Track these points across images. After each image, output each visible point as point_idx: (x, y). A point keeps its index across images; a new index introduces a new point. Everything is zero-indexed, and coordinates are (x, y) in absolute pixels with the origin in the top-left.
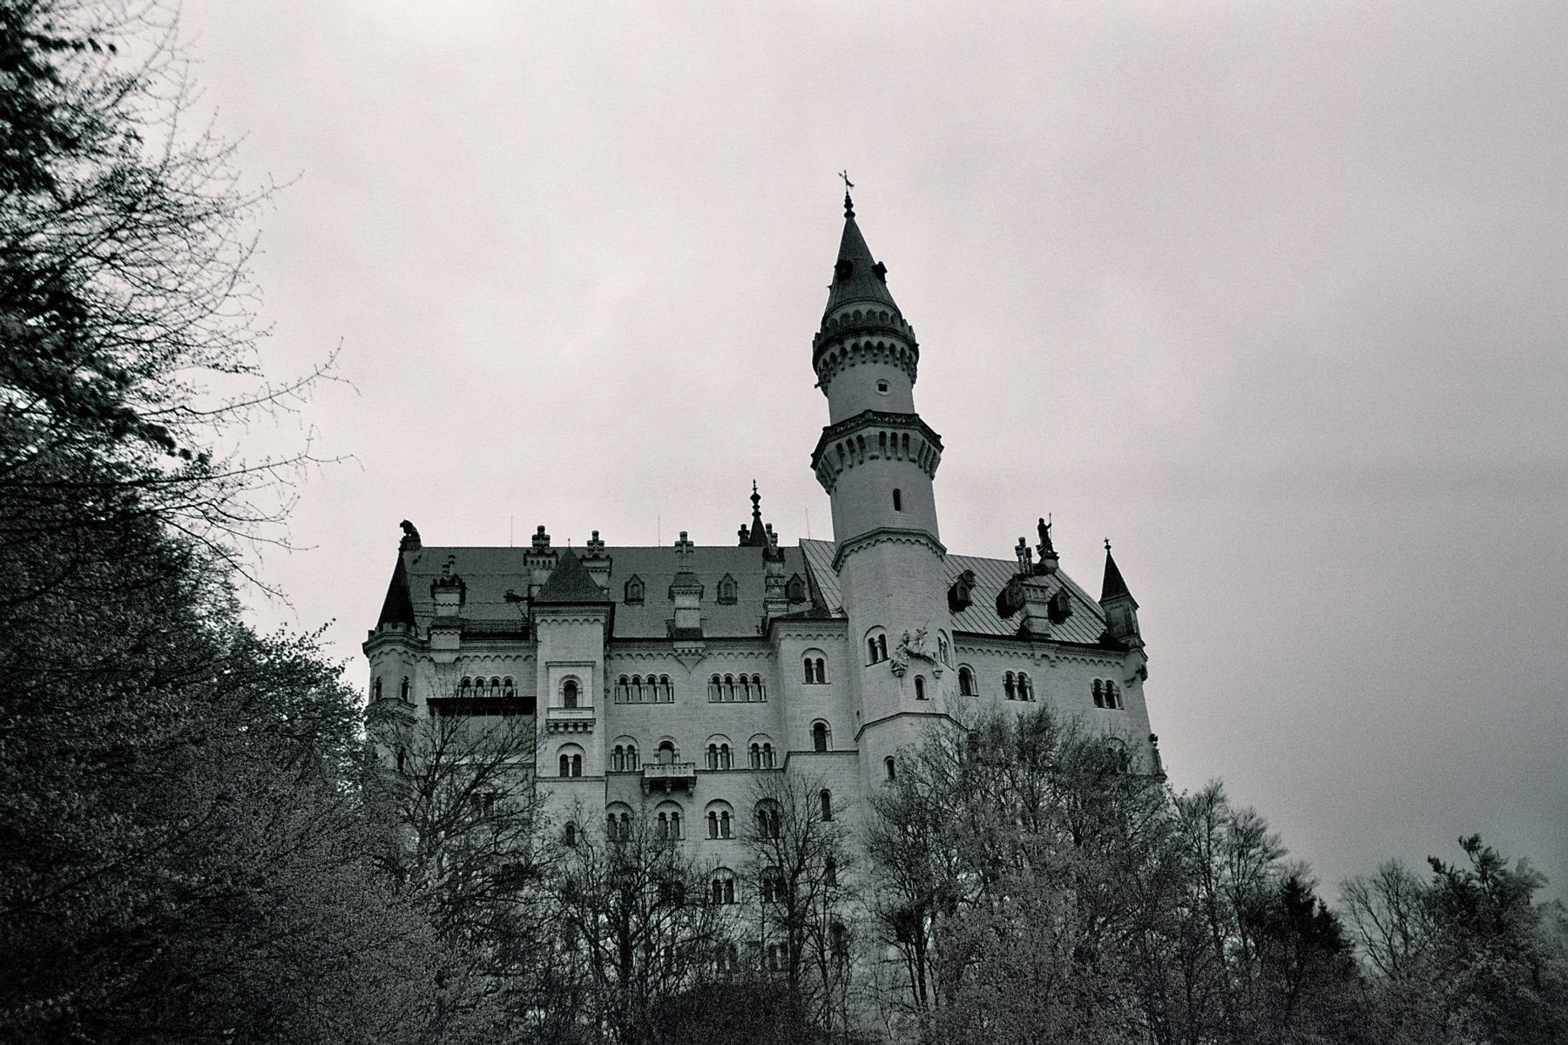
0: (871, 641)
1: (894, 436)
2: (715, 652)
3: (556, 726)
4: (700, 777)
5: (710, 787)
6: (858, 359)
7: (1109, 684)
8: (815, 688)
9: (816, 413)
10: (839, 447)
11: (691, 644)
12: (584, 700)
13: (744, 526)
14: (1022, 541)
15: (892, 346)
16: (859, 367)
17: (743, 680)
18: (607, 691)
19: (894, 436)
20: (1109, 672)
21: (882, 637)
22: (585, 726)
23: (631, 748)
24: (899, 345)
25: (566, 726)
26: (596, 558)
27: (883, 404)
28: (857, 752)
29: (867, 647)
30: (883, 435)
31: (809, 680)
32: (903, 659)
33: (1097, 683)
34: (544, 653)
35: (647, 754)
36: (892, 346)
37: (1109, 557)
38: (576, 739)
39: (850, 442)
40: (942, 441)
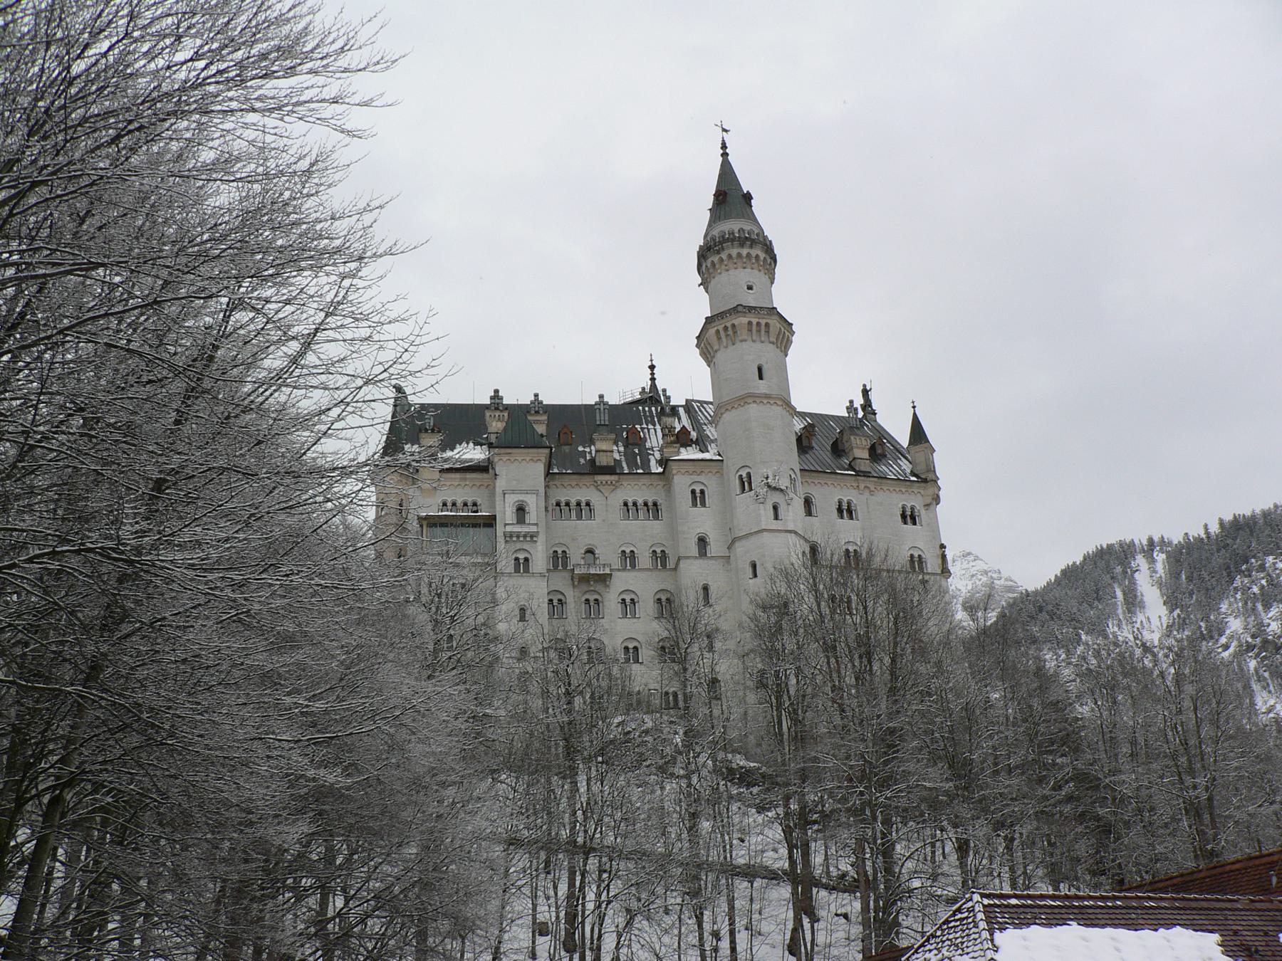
1: (758, 324)
3: (511, 536)
5: (623, 581)
6: (731, 265)
7: (912, 508)
8: (699, 510)
9: (699, 306)
10: (718, 331)
11: (607, 477)
12: (532, 517)
14: (851, 402)
15: (757, 256)
17: (646, 504)
19: (758, 324)
20: (914, 500)
21: (749, 475)
22: (532, 537)
24: (762, 255)
25: (518, 537)
26: (537, 412)
27: (751, 300)
29: (737, 481)
30: (750, 323)
31: (695, 505)
34: (501, 484)
35: (576, 557)
36: (757, 256)
37: (915, 415)
38: (526, 546)
39: (726, 328)
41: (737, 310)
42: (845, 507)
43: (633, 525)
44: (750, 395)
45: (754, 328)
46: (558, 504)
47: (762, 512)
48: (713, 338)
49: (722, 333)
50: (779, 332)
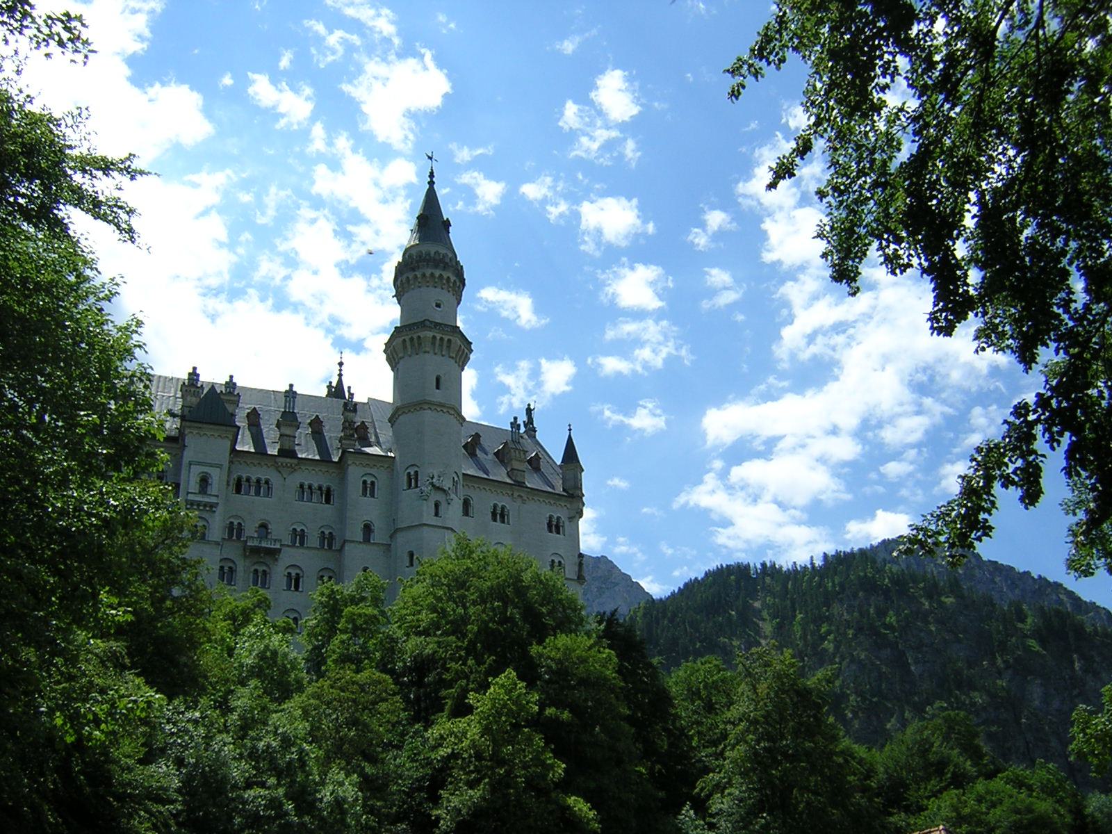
1: (442, 339)
4: (284, 549)
5: (291, 557)
7: (558, 518)
8: (368, 499)
11: (288, 460)
12: (214, 488)
13: (331, 383)
14: (515, 418)
16: (424, 289)
17: (320, 488)
18: (228, 484)
19: (442, 339)
20: (560, 513)
21: (416, 473)
24: (453, 278)
25: (198, 505)
30: (434, 337)
31: (364, 494)
33: (551, 517)
34: (188, 455)
35: (250, 530)
37: (570, 437)
39: (412, 339)
40: (473, 347)
41: (423, 325)
42: (499, 511)
43: (306, 506)
44: (426, 402)
45: (438, 342)
47: (425, 508)
48: (401, 348)
49: (408, 343)
50: (460, 350)
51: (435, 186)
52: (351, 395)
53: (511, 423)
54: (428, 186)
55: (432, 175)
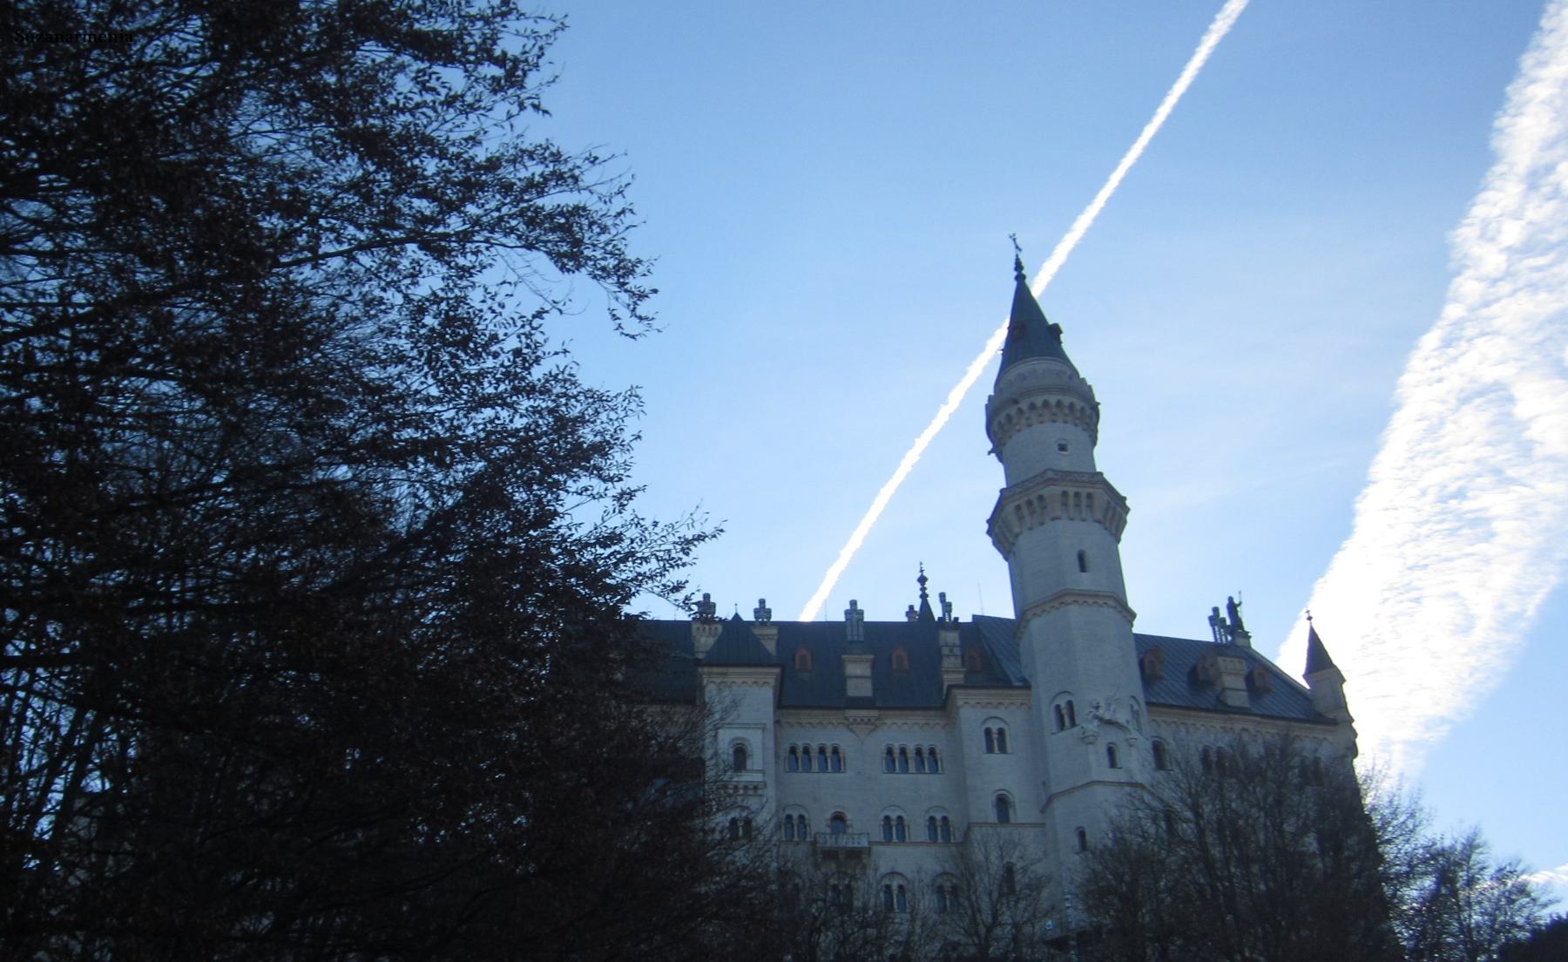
0: (1058, 707)
1: (1077, 495)
2: (889, 722)
4: (876, 849)
8: (997, 757)
9: (992, 478)
10: (1018, 508)
11: (864, 713)
12: (756, 760)
13: (911, 607)
14: (1216, 610)
15: (1071, 406)
17: (919, 752)
18: (777, 756)
19: (1077, 495)
21: (1070, 704)
23: (801, 817)
24: (1079, 404)
27: (1064, 463)
28: (1042, 825)
29: (1053, 715)
30: (1065, 494)
31: (990, 750)
32: (1092, 727)
36: (1071, 406)
43: (904, 782)
46: (793, 751)
49: (1025, 511)
51: (1027, 281)
52: (947, 607)
53: (1211, 619)
54: (1014, 284)
55: (1019, 266)
